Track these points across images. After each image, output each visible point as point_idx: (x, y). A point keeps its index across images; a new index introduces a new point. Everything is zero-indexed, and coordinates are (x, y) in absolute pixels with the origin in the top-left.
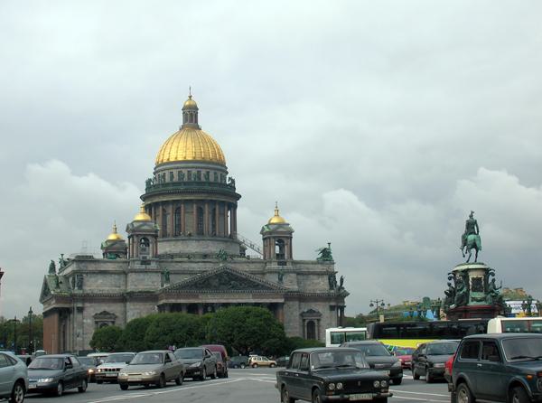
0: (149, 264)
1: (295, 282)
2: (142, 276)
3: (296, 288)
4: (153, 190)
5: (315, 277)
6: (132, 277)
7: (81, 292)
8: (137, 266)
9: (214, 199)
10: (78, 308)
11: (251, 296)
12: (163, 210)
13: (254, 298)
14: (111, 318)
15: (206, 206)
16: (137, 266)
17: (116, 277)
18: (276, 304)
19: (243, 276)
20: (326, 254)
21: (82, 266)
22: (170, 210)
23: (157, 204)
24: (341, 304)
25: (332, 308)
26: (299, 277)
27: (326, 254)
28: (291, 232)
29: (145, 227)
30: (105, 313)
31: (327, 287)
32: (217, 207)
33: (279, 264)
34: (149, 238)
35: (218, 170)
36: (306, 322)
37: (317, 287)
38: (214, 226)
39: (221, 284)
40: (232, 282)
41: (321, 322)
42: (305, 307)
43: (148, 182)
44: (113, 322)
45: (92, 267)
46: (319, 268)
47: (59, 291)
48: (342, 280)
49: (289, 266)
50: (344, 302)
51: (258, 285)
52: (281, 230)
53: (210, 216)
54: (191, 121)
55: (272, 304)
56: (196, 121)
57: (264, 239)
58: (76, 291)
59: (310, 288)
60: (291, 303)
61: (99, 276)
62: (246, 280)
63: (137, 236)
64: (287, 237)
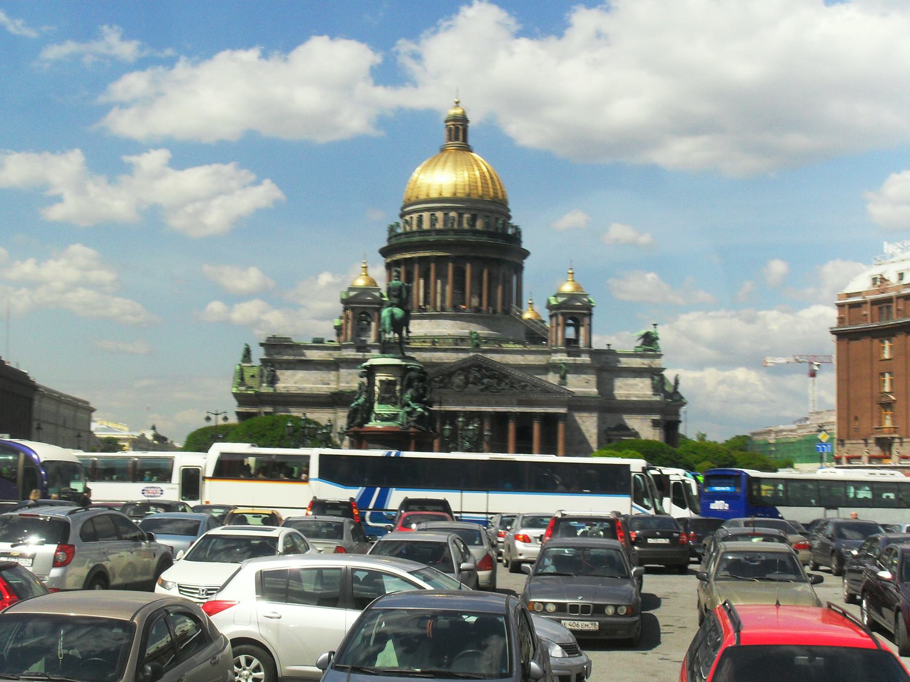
4: (394, 241)
7: (271, 390)
9: (481, 255)
13: (520, 403)
20: (649, 340)
23: (397, 263)
28: (588, 307)
31: (649, 392)
37: (632, 392)
39: (467, 383)
40: (485, 381)
43: (392, 229)
46: (636, 363)
47: (243, 388)
48: (677, 382)
49: (585, 359)
50: (677, 414)
56: (465, 139)
58: (265, 389)
60: (585, 415)
64: (585, 315)
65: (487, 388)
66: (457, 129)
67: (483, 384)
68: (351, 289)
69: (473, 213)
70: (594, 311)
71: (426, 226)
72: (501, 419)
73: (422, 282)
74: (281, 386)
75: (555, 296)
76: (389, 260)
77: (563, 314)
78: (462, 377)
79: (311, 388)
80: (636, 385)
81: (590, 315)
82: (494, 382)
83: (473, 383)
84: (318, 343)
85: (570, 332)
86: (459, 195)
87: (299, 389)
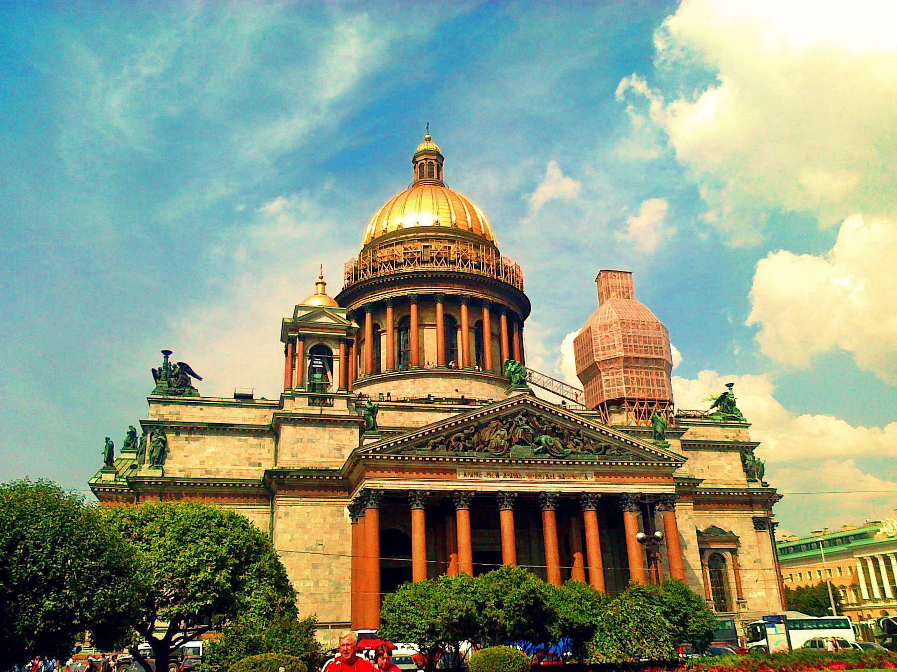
2: (310, 431)
5: (713, 454)
6: (287, 431)
7: (158, 473)
8: (300, 406)
9: (480, 296)
12: (375, 327)
15: (464, 308)
16: (300, 406)
17: (252, 440)
22: (388, 321)
29: (324, 320)
32: (486, 312)
37: (719, 476)
40: (543, 438)
47: (109, 477)
53: (473, 335)
58: (146, 471)
63: (303, 338)
65: (545, 451)
67: (539, 443)
72: (570, 507)
73: (396, 334)
74: (174, 467)
78: (503, 432)
79: (229, 473)
80: (721, 467)
82: (558, 441)
83: (522, 442)
86: (442, 224)
87: (207, 472)
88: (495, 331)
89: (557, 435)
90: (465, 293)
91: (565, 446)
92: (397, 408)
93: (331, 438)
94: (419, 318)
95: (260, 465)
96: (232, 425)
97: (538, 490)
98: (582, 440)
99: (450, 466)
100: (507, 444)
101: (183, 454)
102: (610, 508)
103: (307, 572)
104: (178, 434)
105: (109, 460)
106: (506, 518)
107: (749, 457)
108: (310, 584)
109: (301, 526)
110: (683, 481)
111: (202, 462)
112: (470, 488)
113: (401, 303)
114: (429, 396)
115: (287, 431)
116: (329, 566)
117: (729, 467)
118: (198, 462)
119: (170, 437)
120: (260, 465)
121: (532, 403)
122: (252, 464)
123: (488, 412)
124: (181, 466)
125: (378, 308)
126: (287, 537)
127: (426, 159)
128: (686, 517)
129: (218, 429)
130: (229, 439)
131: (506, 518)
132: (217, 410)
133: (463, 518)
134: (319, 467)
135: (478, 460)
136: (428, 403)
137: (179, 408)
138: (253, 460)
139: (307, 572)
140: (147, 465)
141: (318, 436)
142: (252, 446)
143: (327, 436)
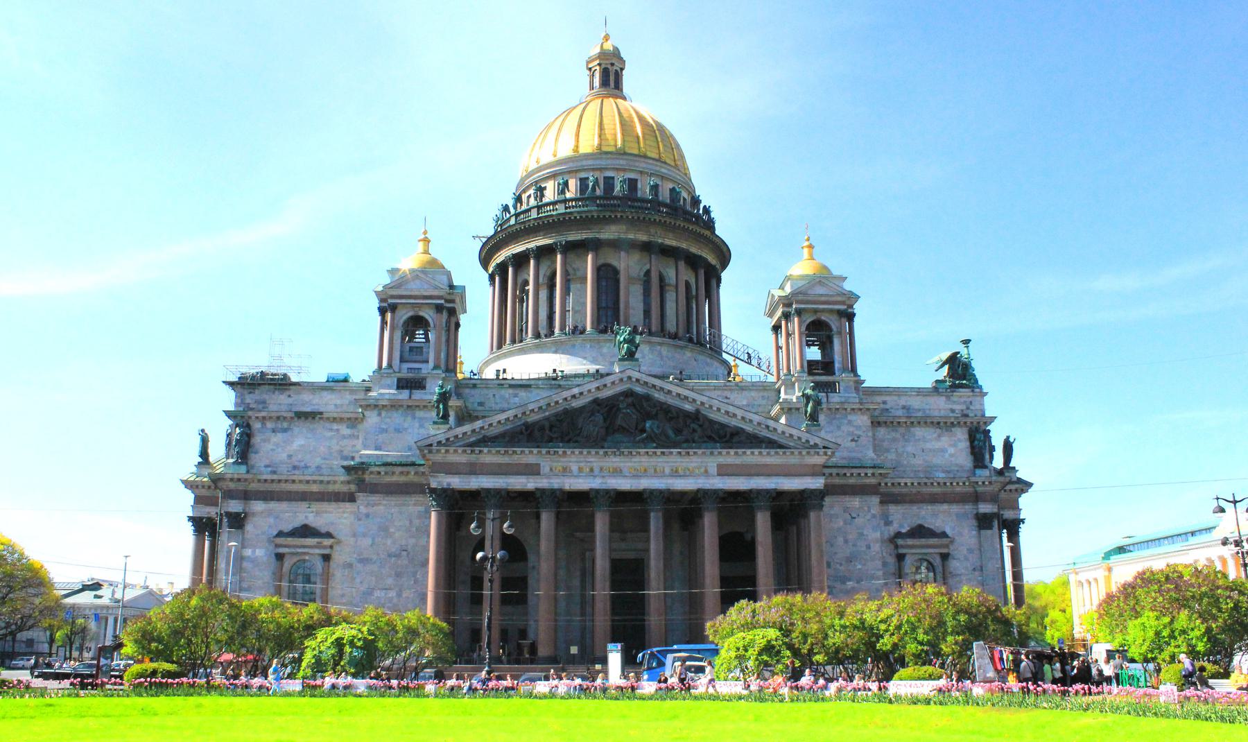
0: (424, 388)
1: (866, 440)
2: (397, 418)
3: (870, 455)
10: (228, 514)
11: (713, 470)
13: (723, 471)
14: (318, 546)
16: (387, 392)
17: (345, 430)
18: (802, 493)
19: (688, 407)
20: (959, 371)
21: (249, 399)
23: (502, 268)
24: (1008, 514)
25: (984, 522)
26: (882, 432)
27: (959, 371)
29: (415, 288)
30: (305, 531)
33: (818, 386)
34: (428, 314)
35: (663, 178)
36: (909, 561)
37: (937, 461)
38: (647, 313)
41: (954, 565)
42: (902, 518)
44: (326, 558)
45: (279, 402)
46: (940, 407)
47: (206, 471)
48: (1008, 448)
50: (1016, 507)
51: (732, 435)
52: (820, 290)
54: (605, 83)
55: (779, 494)
56: (618, 85)
57: (776, 328)
59: (918, 461)
60: (855, 502)
61: (300, 429)
62: (696, 416)
63: (393, 308)
66: (605, 74)
68: (393, 272)
69: (632, 176)
70: (857, 308)
71: (550, 195)
72: (684, 510)
73: (543, 294)
75: (782, 287)
76: (491, 270)
77: (799, 312)
78: (599, 418)
79: (318, 468)
80: (943, 450)
81: (850, 317)
83: (622, 430)
84: (339, 383)
85: (814, 353)
86: (605, 149)
87: (295, 468)
88: (673, 281)
89: (671, 419)
90: (622, 236)
91: (678, 431)
92: (511, 386)
93: (421, 426)
94: (566, 273)
95: (353, 458)
96: (321, 413)
97: (641, 487)
98: (701, 426)
99: (531, 459)
100: (603, 431)
101: (271, 447)
102: (736, 505)
103: (390, 581)
104: (264, 424)
105: (204, 454)
106: (601, 523)
107: (980, 436)
108: (392, 594)
109: (384, 529)
110: (862, 472)
111: (290, 456)
112: (556, 486)
113: (544, 253)
114: (555, 371)
115: (372, 418)
116: (415, 574)
117: (951, 450)
118: (284, 456)
119: (257, 425)
120: (353, 458)
121: (638, 380)
122: (346, 458)
123: (581, 394)
124: (267, 462)
125: (520, 261)
126: (369, 541)
127: (599, 64)
128: (868, 517)
129: (306, 418)
130: (319, 427)
131: (601, 523)
132: (306, 397)
133: (547, 520)
134: (404, 460)
135: (565, 453)
136: (555, 381)
137: (266, 396)
138: (345, 453)
139: (390, 581)
140: (231, 461)
141: (406, 425)
142: (344, 437)
143: (417, 425)
